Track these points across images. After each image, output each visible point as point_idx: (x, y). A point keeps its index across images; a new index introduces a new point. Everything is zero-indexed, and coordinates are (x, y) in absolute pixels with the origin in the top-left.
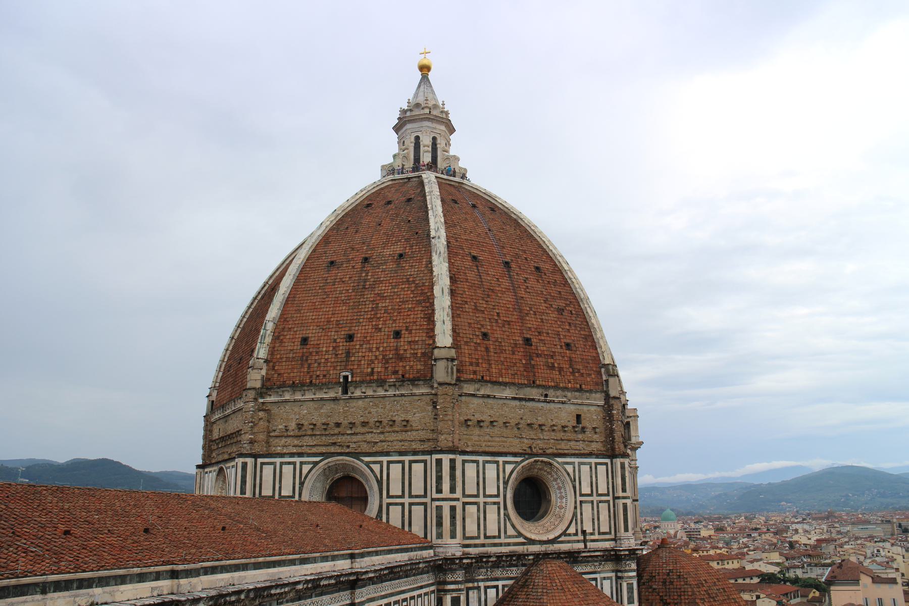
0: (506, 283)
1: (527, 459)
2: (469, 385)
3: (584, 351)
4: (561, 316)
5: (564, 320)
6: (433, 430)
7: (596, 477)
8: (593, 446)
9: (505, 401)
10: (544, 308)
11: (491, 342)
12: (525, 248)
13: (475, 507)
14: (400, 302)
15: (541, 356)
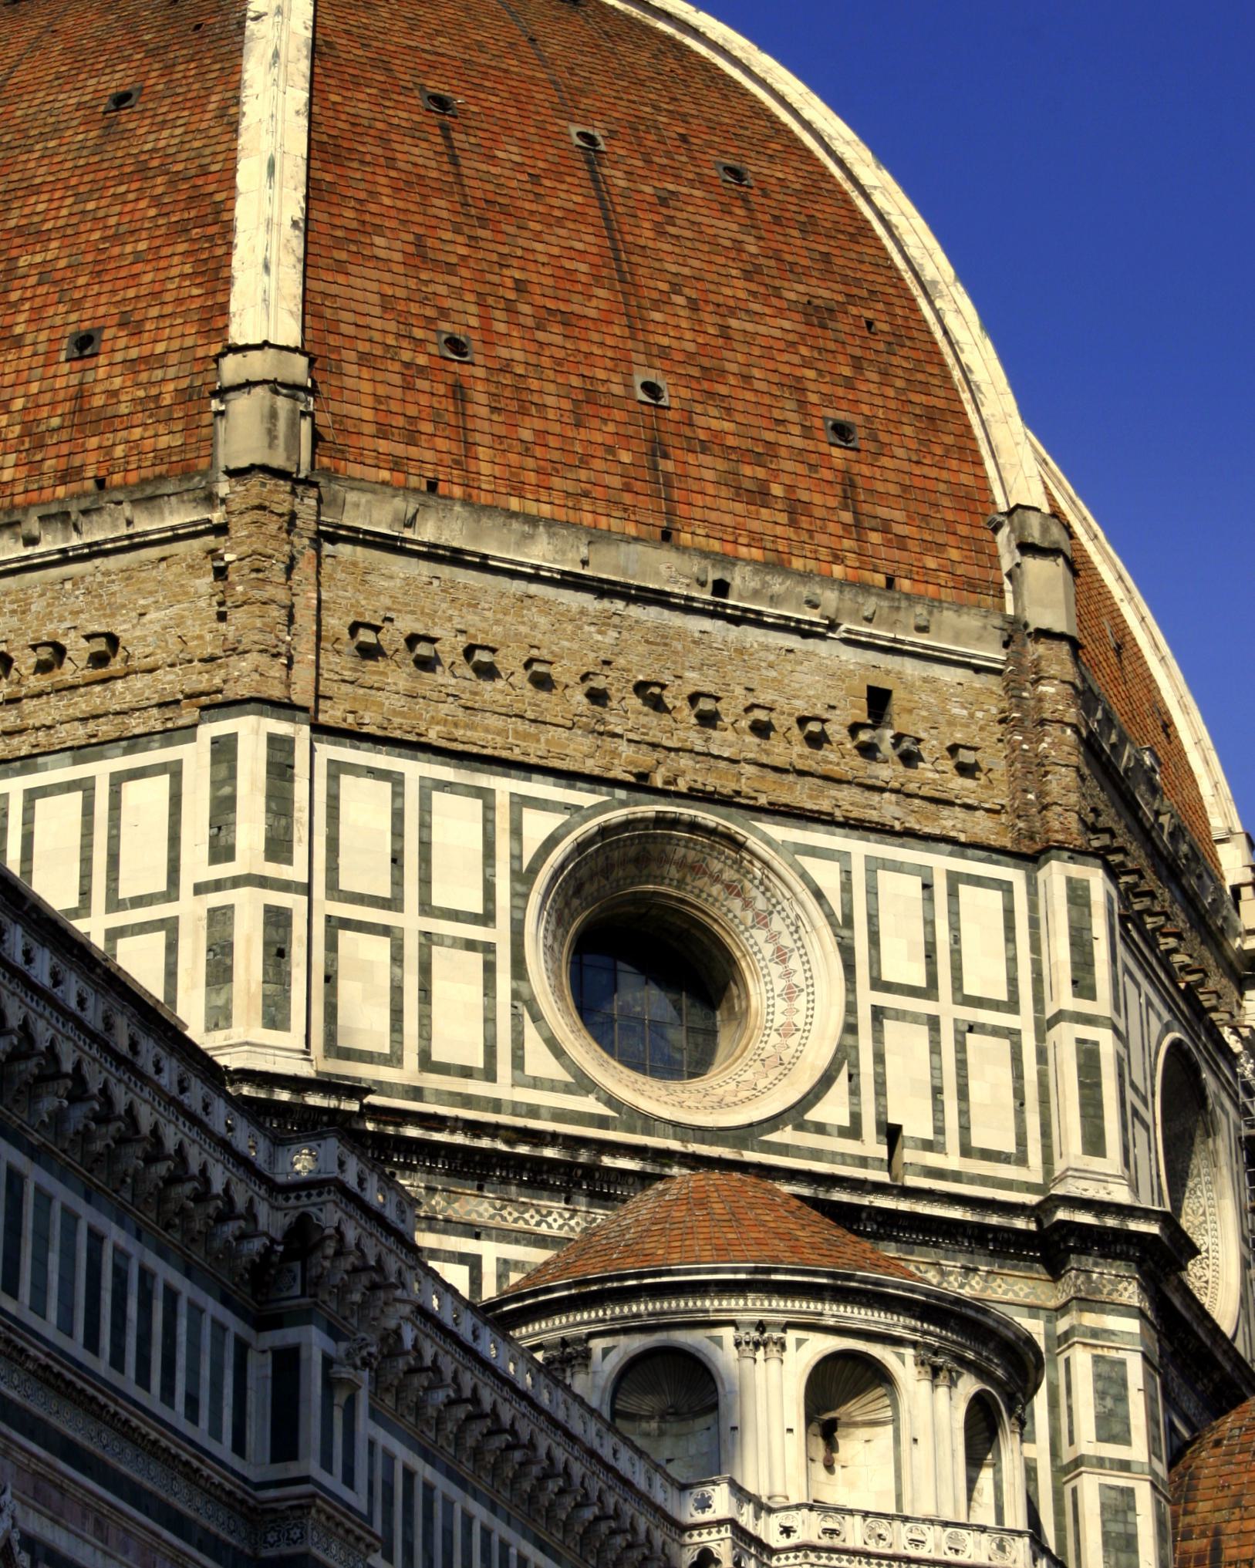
0: (571, 194)
1: (623, 804)
2: (369, 496)
3: (918, 463)
4: (819, 332)
5: (832, 346)
6: (212, 659)
7: (955, 928)
8: (949, 823)
9: (534, 588)
10: (742, 294)
11: (480, 372)
12: (689, 108)
13: (384, 944)
14: (104, 239)
15: (705, 448)
